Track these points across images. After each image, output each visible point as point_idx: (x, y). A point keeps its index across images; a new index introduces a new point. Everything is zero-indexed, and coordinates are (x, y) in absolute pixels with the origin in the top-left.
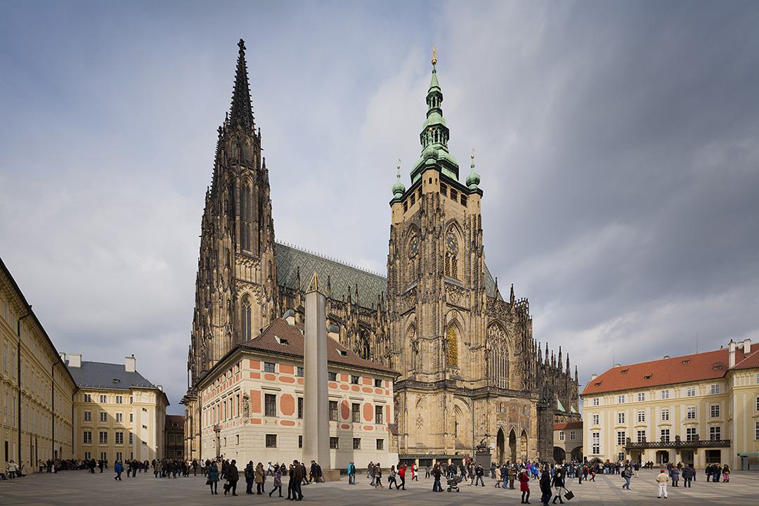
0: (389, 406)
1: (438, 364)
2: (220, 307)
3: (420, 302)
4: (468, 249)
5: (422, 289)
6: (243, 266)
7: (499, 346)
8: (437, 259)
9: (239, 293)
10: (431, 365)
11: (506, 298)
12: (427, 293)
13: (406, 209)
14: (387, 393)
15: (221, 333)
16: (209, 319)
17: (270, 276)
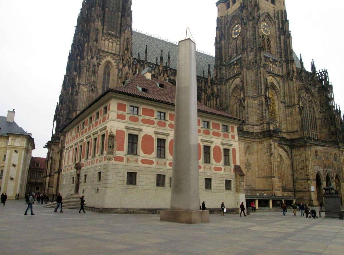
0: (235, 149)
1: (262, 118)
2: (87, 70)
3: (245, 69)
4: (278, 33)
5: (246, 59)
6: (107, 42)
7: (308, 105)
8: (257, 38)
9: (102, 60)
10: (255, 118)
11: (308, 69)
12: (250, 62)
13: (228, 7)
14: (233, 137)
15: (86, 90)
16: (77, 79)
17: (127, 49)
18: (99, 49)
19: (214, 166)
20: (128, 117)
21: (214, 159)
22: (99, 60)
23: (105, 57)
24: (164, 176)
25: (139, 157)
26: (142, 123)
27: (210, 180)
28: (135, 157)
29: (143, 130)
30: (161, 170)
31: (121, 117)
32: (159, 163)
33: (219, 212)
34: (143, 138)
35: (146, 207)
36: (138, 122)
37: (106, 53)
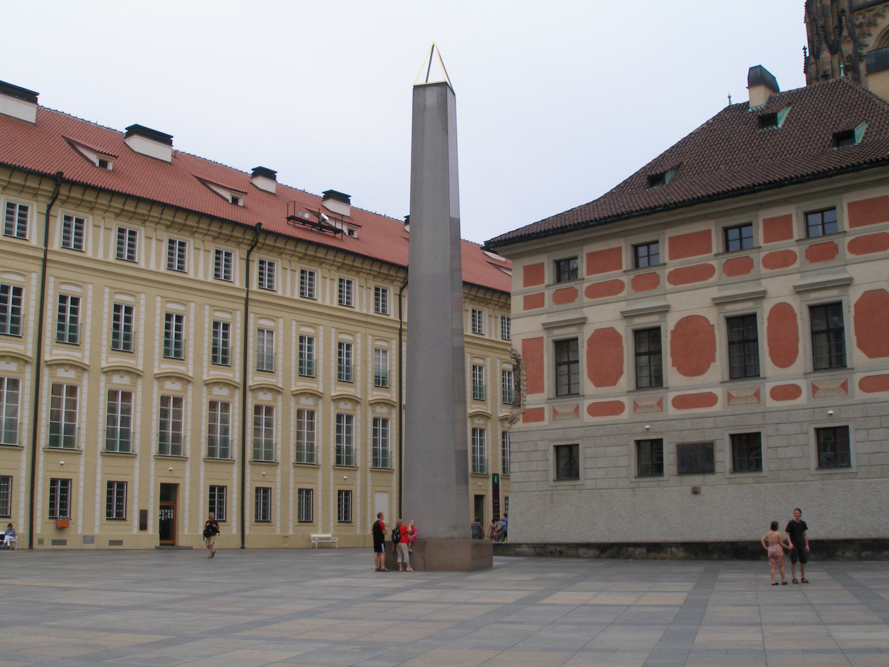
18: (843, 11)
19: (864, 375)
20: (551, 296)
21: (860, 345)
22: (847, 48)
23: (872, 24)
24: (660, 441)
25: (582, 398)
26: (587, 300)
27: (843, 431)
28: (573, 401)
29: (590, 320)
30: (647, 427)
31: (533, 302)
32: (639, 404)
33: (864, 553)
34: (591, 341)
35: (592, 540)
36: (576, 300)
37: (873, 9)
